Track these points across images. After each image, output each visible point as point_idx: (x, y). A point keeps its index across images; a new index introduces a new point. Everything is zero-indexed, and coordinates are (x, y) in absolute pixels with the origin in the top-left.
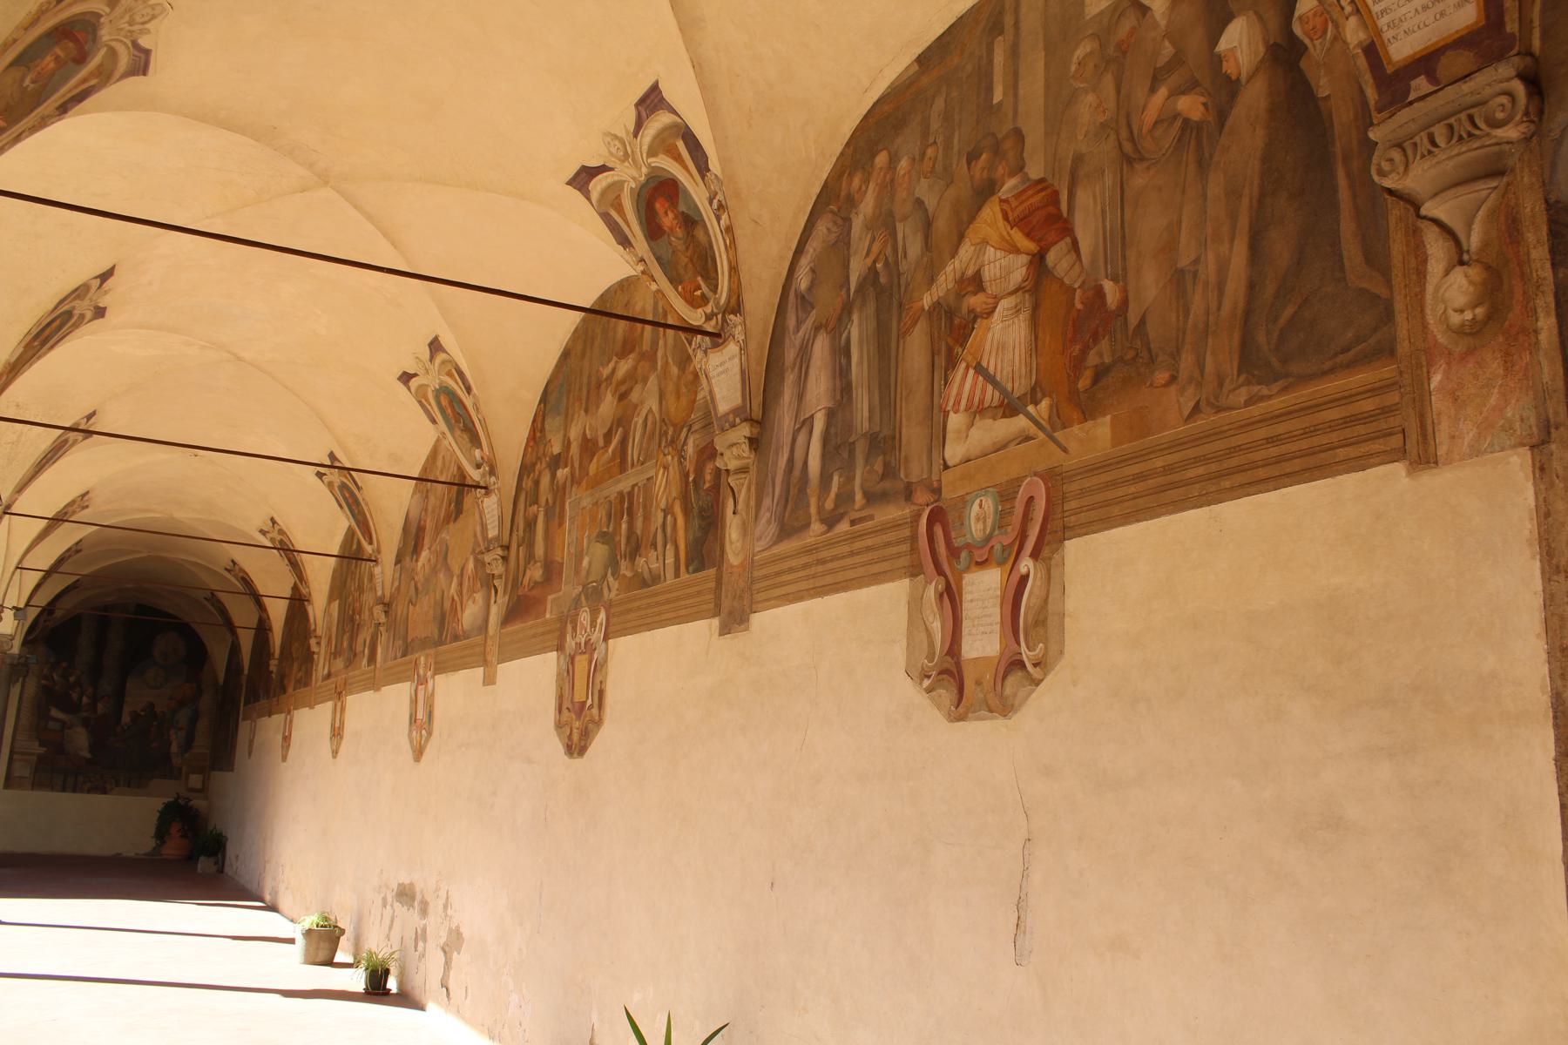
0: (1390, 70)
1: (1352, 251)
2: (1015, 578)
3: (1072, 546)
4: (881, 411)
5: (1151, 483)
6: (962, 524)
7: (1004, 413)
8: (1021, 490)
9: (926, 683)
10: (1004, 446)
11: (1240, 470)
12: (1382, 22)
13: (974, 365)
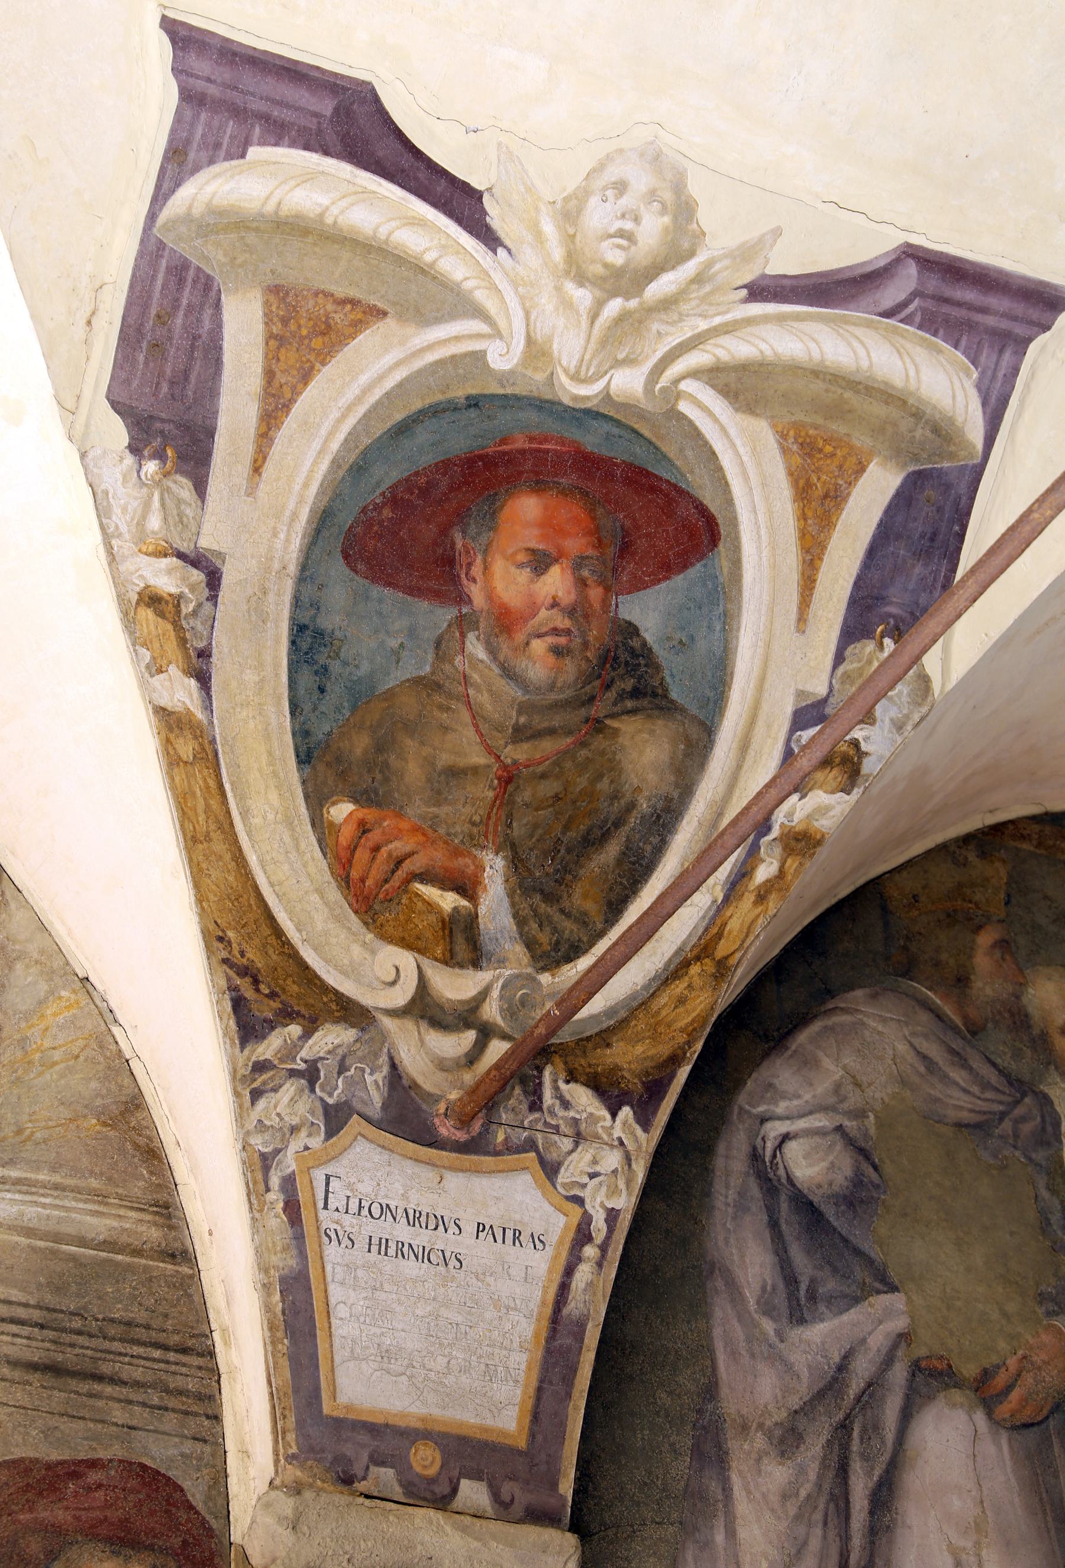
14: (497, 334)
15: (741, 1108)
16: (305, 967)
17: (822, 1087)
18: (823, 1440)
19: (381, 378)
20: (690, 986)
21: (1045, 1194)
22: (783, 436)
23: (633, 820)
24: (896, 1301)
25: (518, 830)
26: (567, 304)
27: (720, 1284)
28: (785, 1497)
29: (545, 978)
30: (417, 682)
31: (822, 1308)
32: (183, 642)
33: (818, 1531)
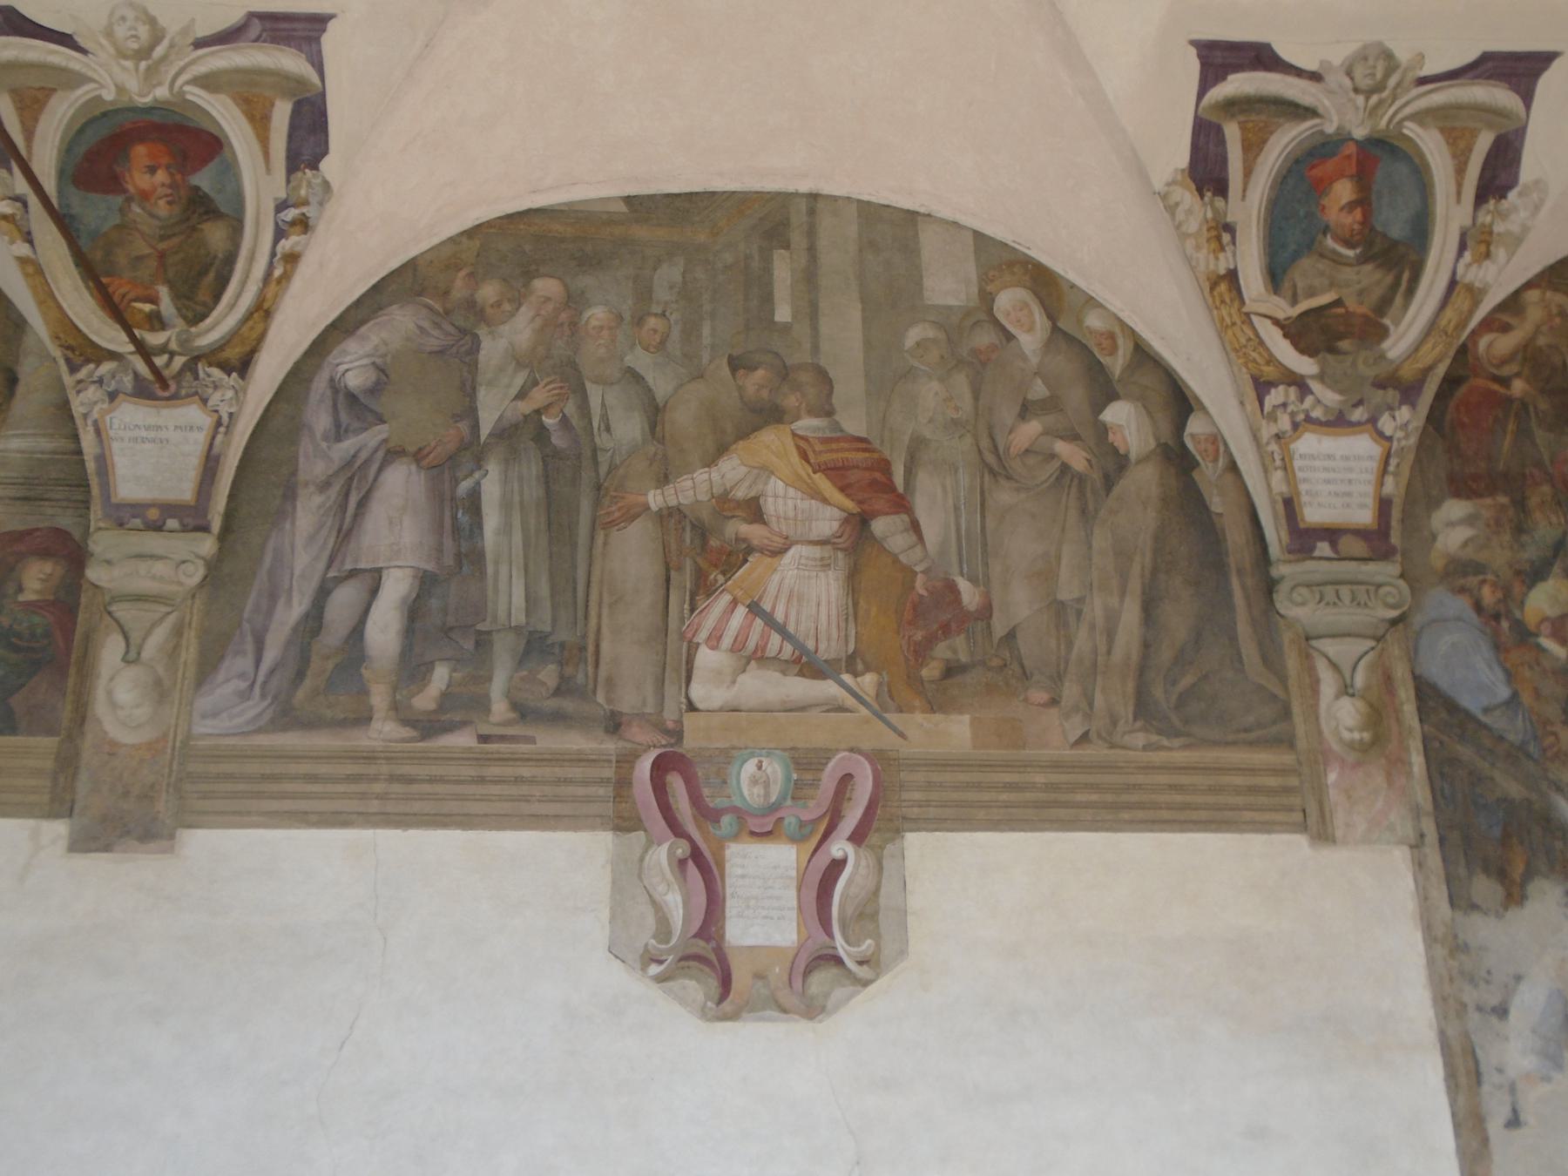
0: (1302, 526)
1: (1249, 651)
2: (822, 862)
3: (914, 841)
4: (555, 607)
5: (1029, 796)
6: (725, 782)
7: (801, 670)
8: (831, 764)
9: (654, 969)
10: (803, 709)
11: (1140, 806)
12: (1303, 487)
13: (748, 602)
14: (102, 86)
16: (91, 341)
17: (368, 347)
19: (64, 115)
20: (255, 323)
21: (465, 374)
22: (234, 100)
23: (217, 262)
24: (385, 427)
25: (171, 274)
26: (124, 69)
28: (320, 507)
29: (193, 330)
30: (117, 227)
32: (19, 230)
33: (331, 519)
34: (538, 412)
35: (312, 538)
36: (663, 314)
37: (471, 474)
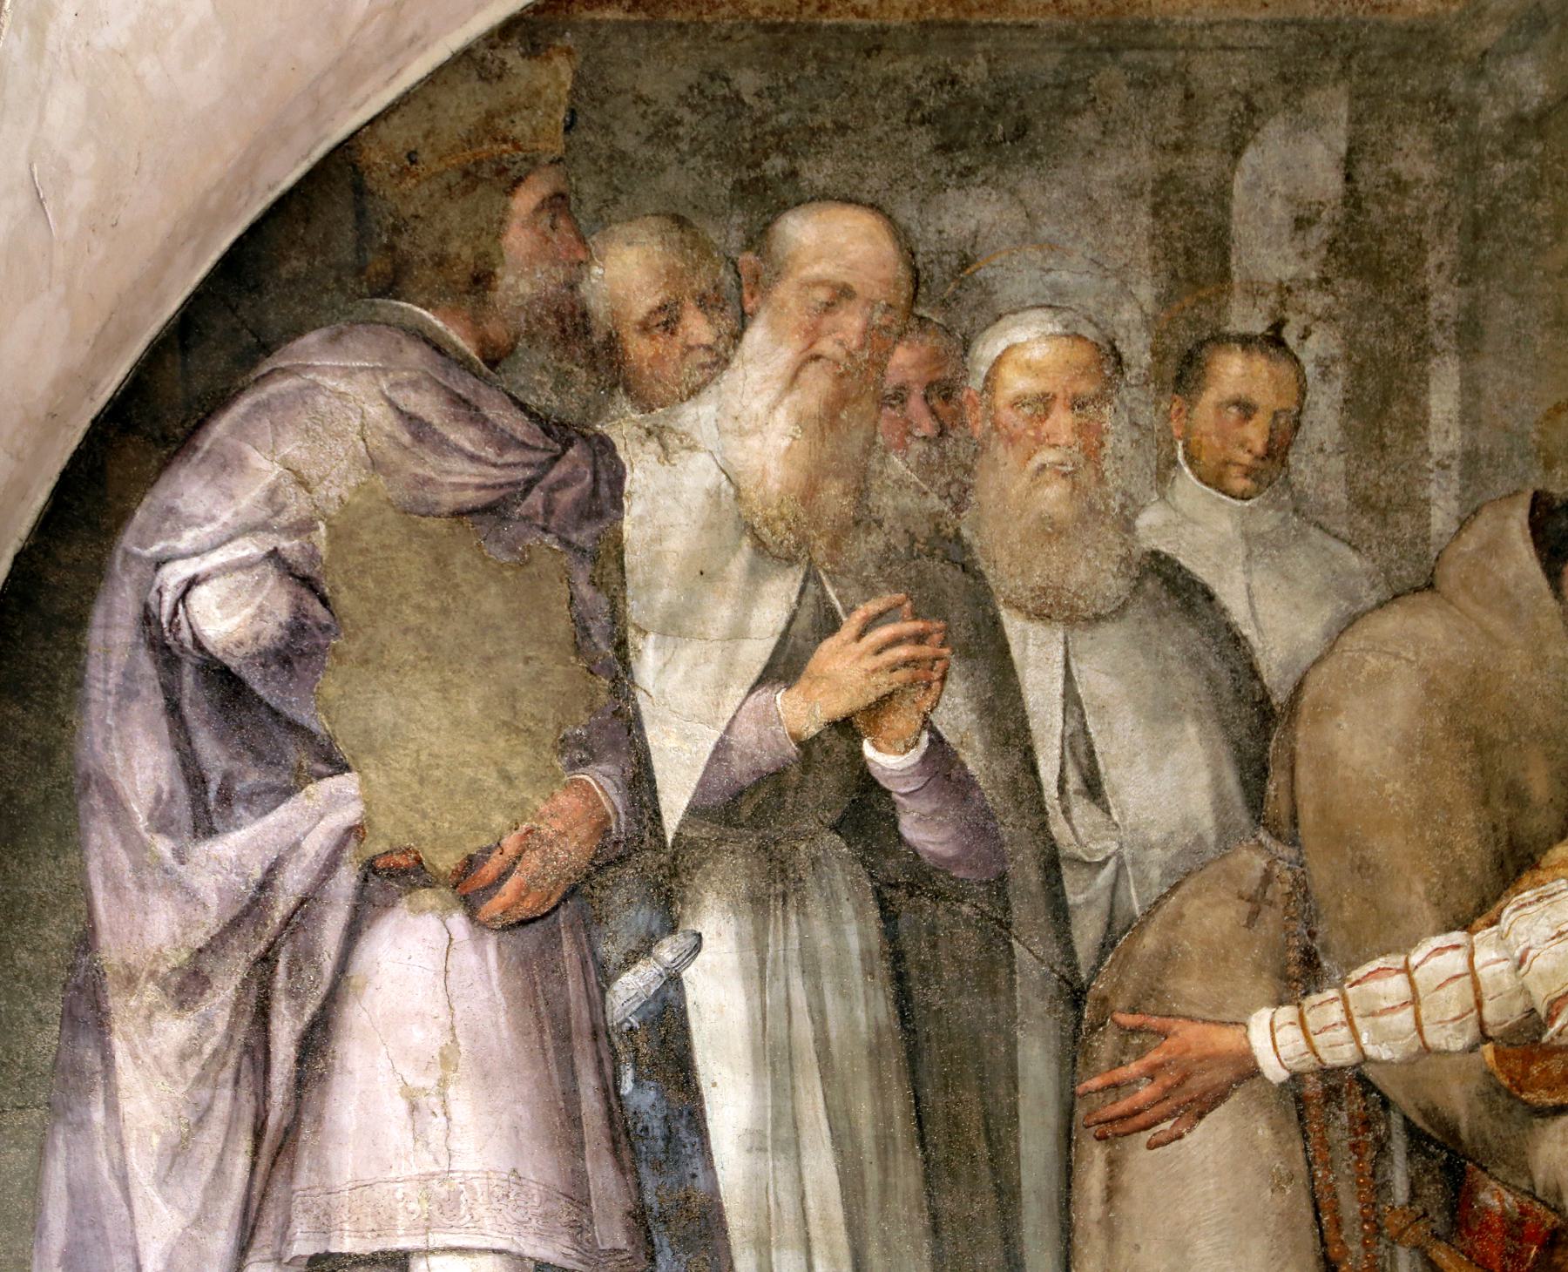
15: (127, 553)
18: (236, 981)
21: (585, 591)
24: (347, 783)
27: (97, 801)
28: (183, 1057)
31: (239, 810)
33: (227, 1092)
34: (845, 727)
35: (177, 1155)
36: (1274, 340)
37: (645, 948)
